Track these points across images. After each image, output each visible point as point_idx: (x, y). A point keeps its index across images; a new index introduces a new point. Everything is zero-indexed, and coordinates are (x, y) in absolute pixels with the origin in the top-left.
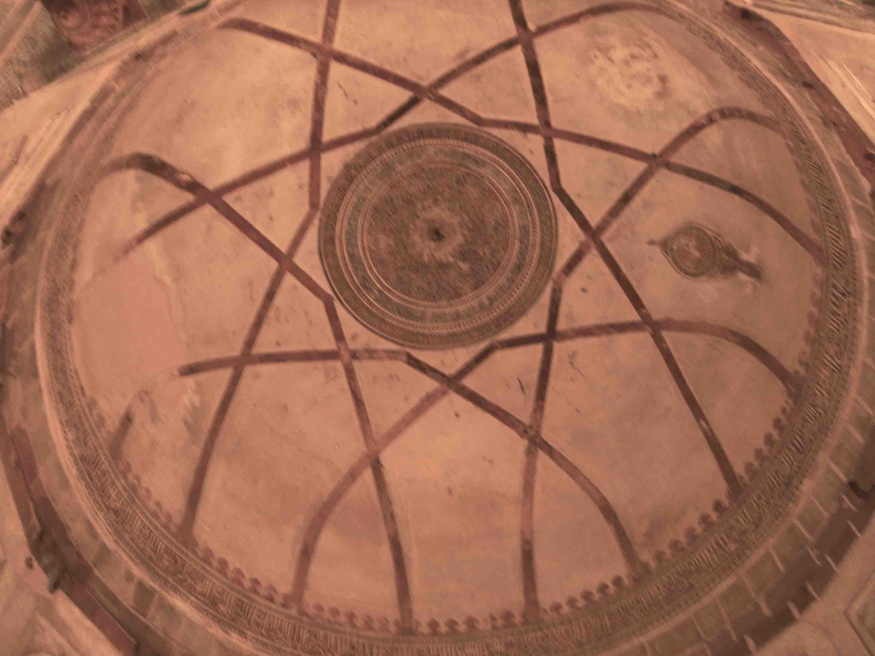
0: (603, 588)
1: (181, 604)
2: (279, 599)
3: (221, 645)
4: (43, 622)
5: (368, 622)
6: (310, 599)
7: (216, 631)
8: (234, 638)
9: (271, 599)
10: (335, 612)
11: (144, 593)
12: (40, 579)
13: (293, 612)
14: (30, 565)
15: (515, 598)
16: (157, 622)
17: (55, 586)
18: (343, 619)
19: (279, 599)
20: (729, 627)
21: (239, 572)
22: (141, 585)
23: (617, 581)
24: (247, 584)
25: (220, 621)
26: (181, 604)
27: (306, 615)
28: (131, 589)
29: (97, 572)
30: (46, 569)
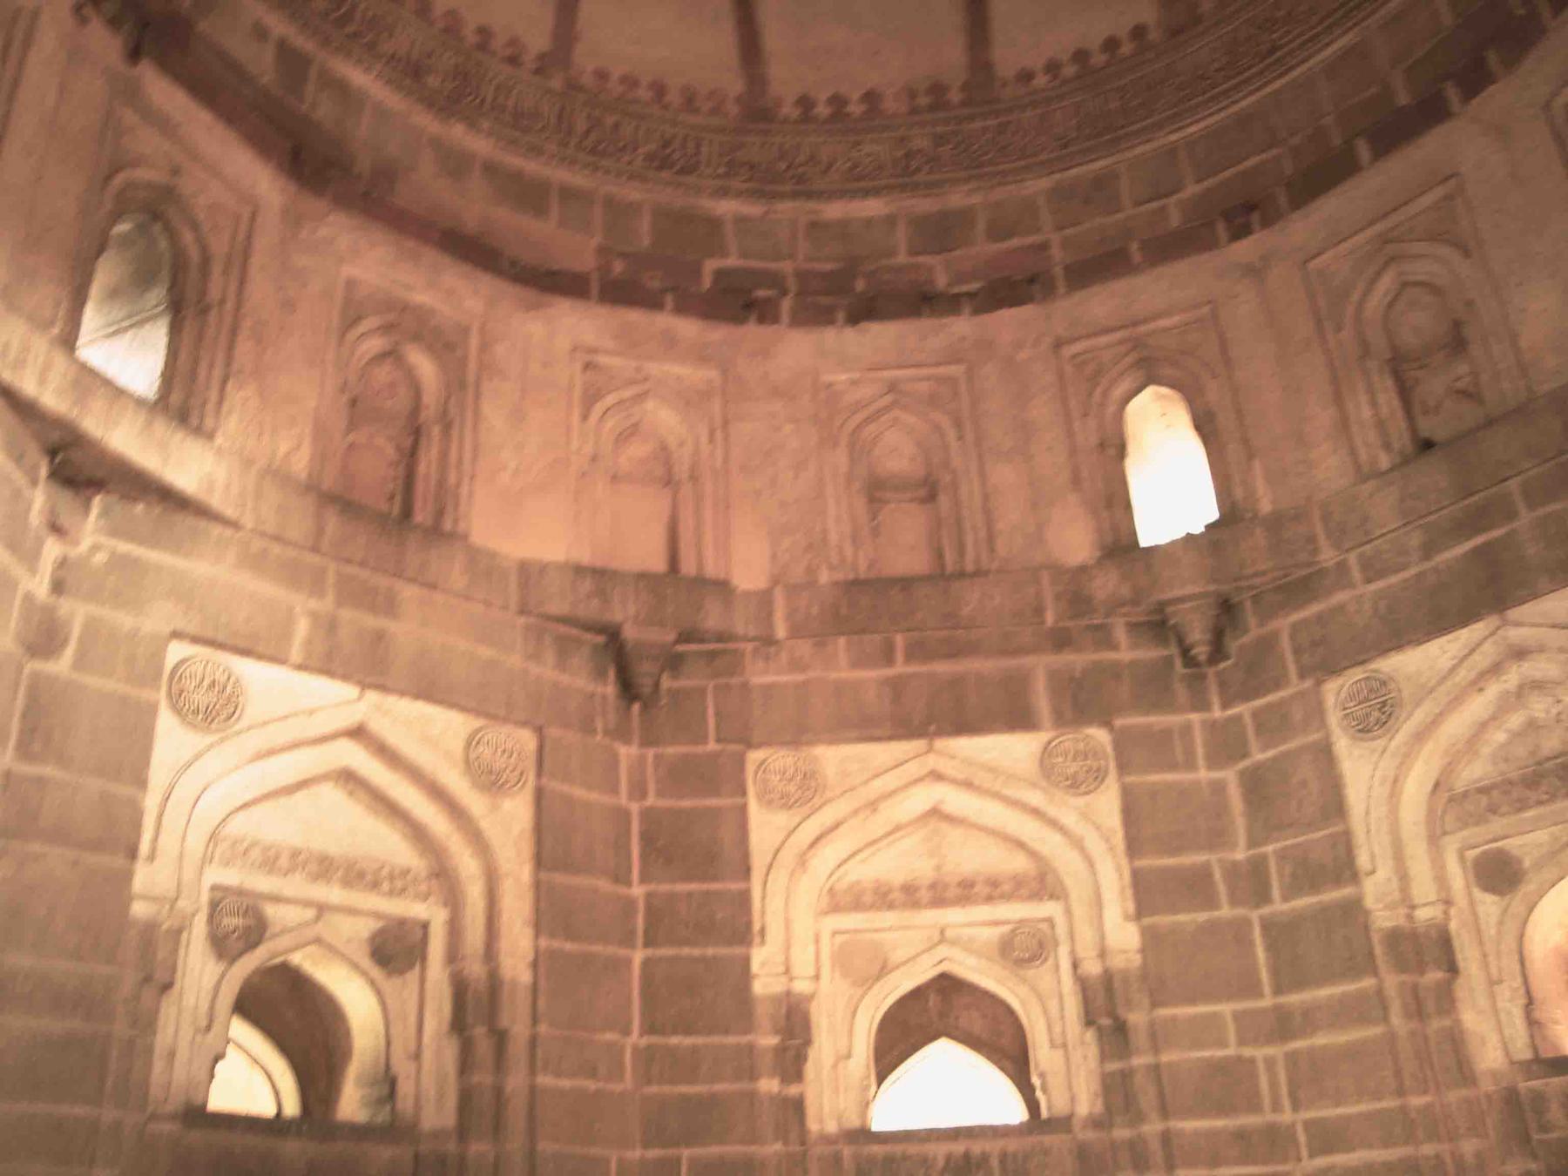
0: (1111, 44)
1: (359, 77)
2: (529, 60)
3: (436, 143)
4: (129, 117)
5: (690, 101)
6: (585, 60)
7: (426, 122)
8: (457, 133)
9: (513, 60)
10: (630, 82)
11: (292, 63)
12: (105, 43)
13: (556, 83)
14: (83, 21)
15: (952, 59)
16: (324, 110)
17: (135, 54)
18: (643, 93)
19: (529, 60)
20: (1328, 120)
21: (452, 15)
22: (283, 47)
23: (1138, 32)
24: (470, 35)
25: (430, 102)
26: (359, 77)
27: (580, 89)
28: (269, 54)
29: (203, 26)
30: (114, 23)
